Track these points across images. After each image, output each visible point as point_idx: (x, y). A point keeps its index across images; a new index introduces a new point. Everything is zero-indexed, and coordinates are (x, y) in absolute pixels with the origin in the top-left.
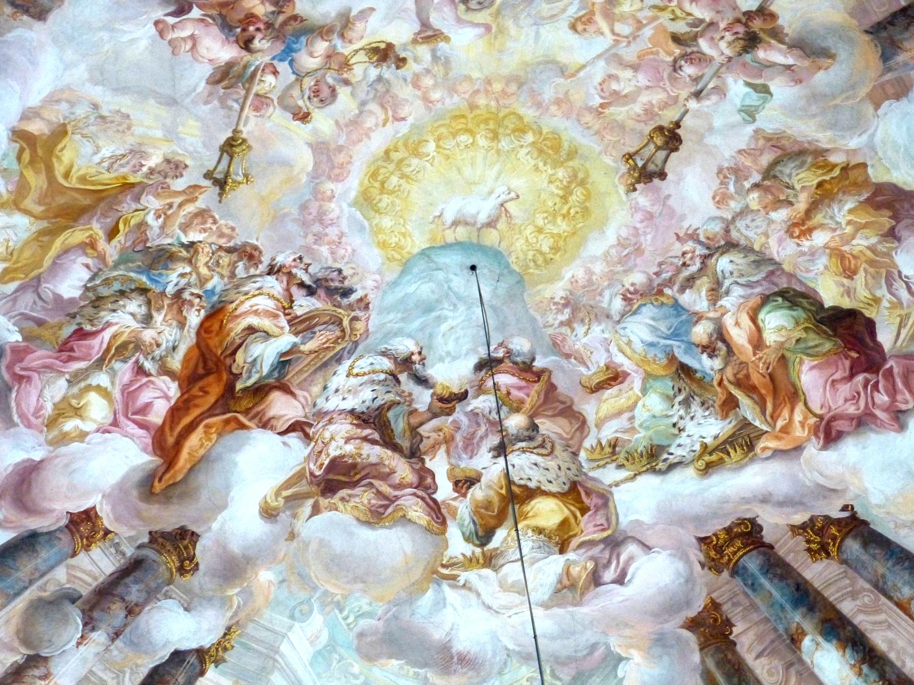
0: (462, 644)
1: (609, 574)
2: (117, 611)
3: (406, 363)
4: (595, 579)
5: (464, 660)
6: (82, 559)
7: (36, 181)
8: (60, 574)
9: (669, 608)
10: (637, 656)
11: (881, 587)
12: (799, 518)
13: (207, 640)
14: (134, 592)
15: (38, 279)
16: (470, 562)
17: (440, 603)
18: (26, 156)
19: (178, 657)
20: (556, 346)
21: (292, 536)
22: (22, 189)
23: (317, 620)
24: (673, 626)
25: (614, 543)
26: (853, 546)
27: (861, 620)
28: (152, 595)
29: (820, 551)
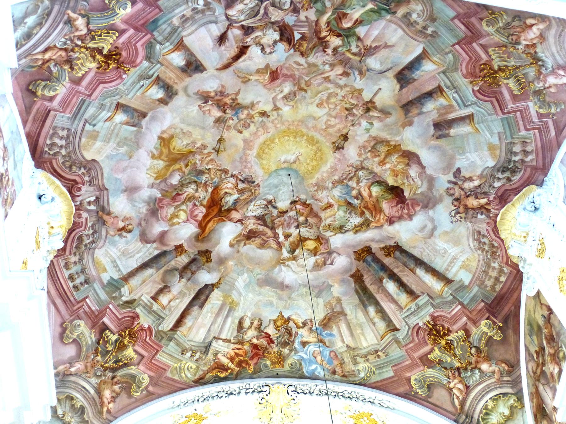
0: (287, 281)
1: (329, 262)
2: (189, 274)
3: (270, 202)
4: (325, 264)
5: (288, 287)
6: (179, 258)
7: (165, 151)
8: (173, 263)
9: (346, 271)
10: (336, 285)
11: (405, 265)
12: (382, 246)
13: (214, 281)
14: (194, 268)
15: (166, 179)
16: (289, 259)
17: (281, 271)
18: (162, 144)
19: (206, 286)
20: (313, 197)
21: (238, 252)
22: (161, 153)
23: (246, 275)
24: (347, 276)
25: (330, 253)
26: (397, 253)
27: (400, 274)
28: (199, 268)
29: (388, 255)
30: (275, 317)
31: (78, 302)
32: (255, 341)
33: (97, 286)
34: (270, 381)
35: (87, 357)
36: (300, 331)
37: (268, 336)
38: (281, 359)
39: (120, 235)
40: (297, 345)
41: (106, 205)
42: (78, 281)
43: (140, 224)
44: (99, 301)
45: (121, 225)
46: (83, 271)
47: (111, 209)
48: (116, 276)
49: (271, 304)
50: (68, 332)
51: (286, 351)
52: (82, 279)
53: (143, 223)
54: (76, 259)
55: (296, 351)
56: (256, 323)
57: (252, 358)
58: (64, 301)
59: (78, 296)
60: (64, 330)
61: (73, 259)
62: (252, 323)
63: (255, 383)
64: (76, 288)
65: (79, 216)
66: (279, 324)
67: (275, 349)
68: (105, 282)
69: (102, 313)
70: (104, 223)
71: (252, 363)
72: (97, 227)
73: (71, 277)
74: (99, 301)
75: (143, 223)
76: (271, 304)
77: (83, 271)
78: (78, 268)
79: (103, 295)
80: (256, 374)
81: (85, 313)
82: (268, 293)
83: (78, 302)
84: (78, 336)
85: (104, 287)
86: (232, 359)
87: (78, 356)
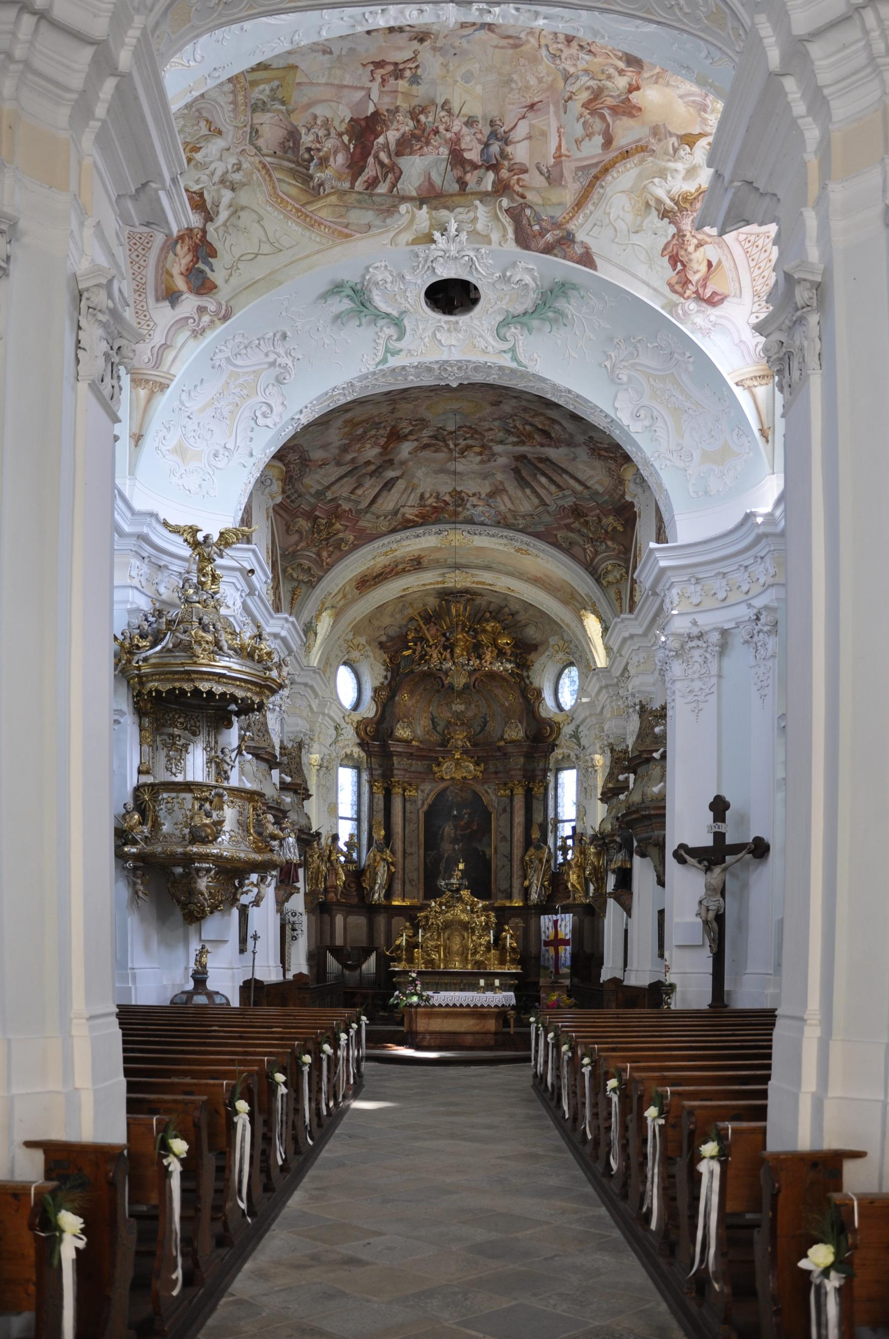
3: (441, 428)
20: (476, 424)
30: (450, 490)
32: (434, 504)
34: (447, 526)
36: (471, 499)
37: (445, 501)
38: (456, 514)
40: (468, 506)
49: (446, 483)
51: (460, 509)
55: (468, 510)
56: (434, 494)
57: (433, 514)
62: (431, 495)
63: (435, 528)
66: (453, 494)
67: (451, 508)
71: (433, 516)
76: (446, 483)
80: (437, 522)
82: (443, 477)
86: (417, 516)
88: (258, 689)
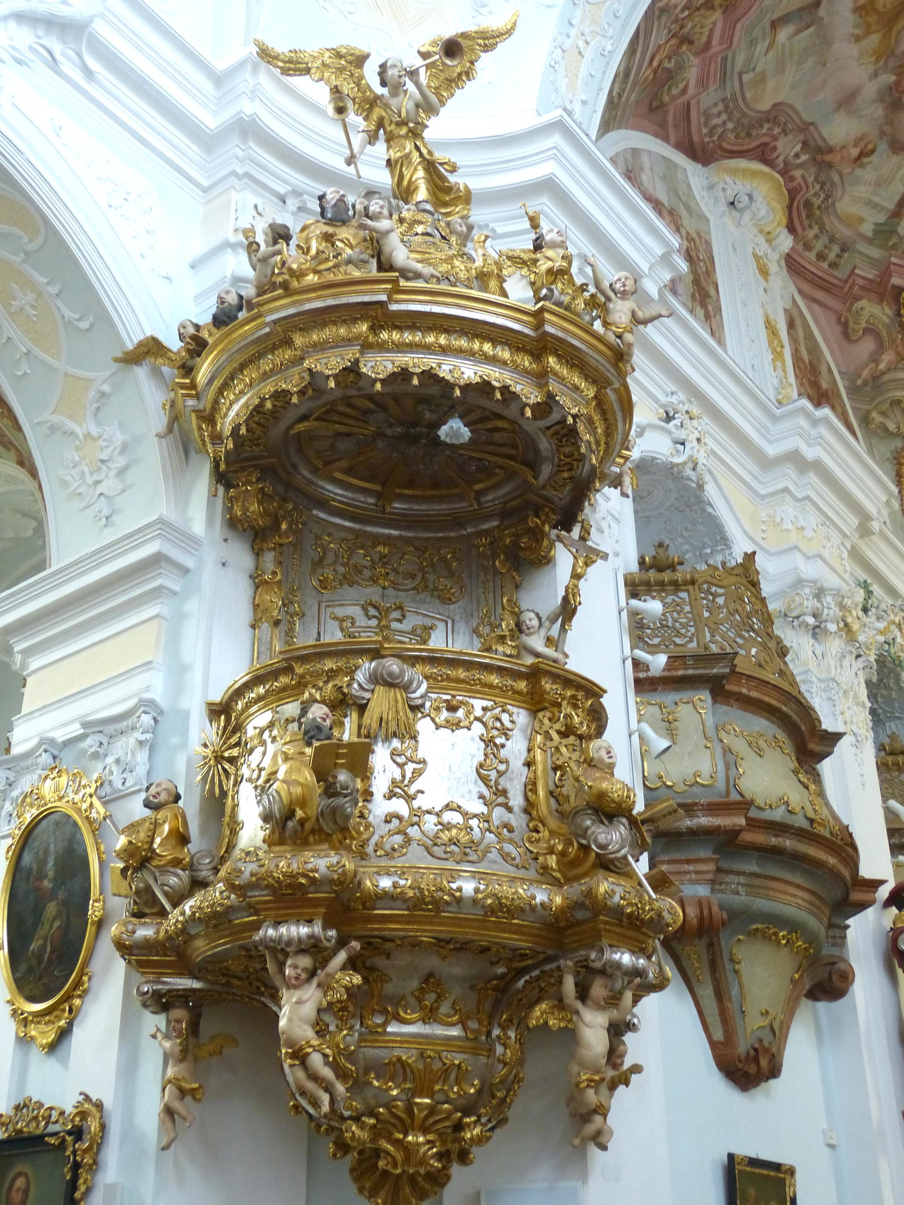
7: (873, 19)
15: (892, 52)
18: (863, 13)
22: (868, 25)
31: (846, 281)
33: (861, 246)
35: (893, 341)
39: (862, 166)
41: (821, 143)
42: (832, 256)
43: (882, 134)
44: (873, 263)
45: (855, 152)
46: (832, 240)
47: (831, 143)
48: (881, 218)
50: (851, 324)
52: (836, 249)
53: (887, 129)
54: (816, 230)
58: (827, 291)
59: (842, 273)
60: (845, 326)
61: (811, 234)
64: (834, 265)
65: (792, 179)
68: (870, 234)
69: (886, 274)
70: (830, 165)
72: (823, 177)
73: (821, 256)
74: (873, 263)
75: (887, 129)
77: (832, 240)
78: (824, 239)
79: (875, 253)
81: (862, 288)
83: (846, 281)
84: (868, 322)
85: (870, 241)
87: (881, 347)
88: (526, 362)
